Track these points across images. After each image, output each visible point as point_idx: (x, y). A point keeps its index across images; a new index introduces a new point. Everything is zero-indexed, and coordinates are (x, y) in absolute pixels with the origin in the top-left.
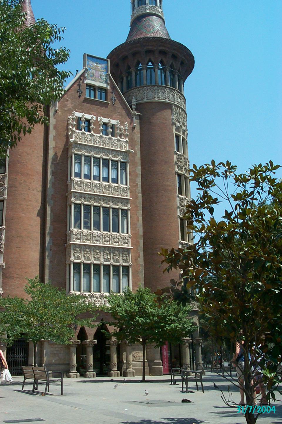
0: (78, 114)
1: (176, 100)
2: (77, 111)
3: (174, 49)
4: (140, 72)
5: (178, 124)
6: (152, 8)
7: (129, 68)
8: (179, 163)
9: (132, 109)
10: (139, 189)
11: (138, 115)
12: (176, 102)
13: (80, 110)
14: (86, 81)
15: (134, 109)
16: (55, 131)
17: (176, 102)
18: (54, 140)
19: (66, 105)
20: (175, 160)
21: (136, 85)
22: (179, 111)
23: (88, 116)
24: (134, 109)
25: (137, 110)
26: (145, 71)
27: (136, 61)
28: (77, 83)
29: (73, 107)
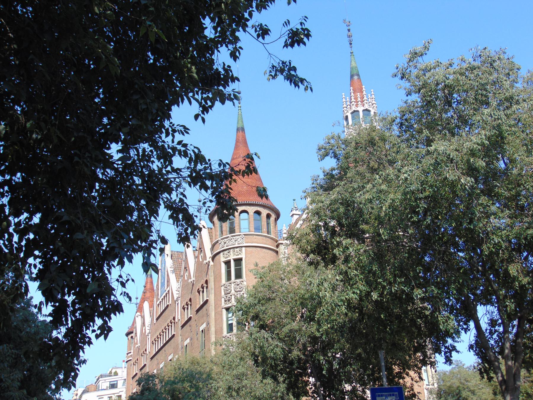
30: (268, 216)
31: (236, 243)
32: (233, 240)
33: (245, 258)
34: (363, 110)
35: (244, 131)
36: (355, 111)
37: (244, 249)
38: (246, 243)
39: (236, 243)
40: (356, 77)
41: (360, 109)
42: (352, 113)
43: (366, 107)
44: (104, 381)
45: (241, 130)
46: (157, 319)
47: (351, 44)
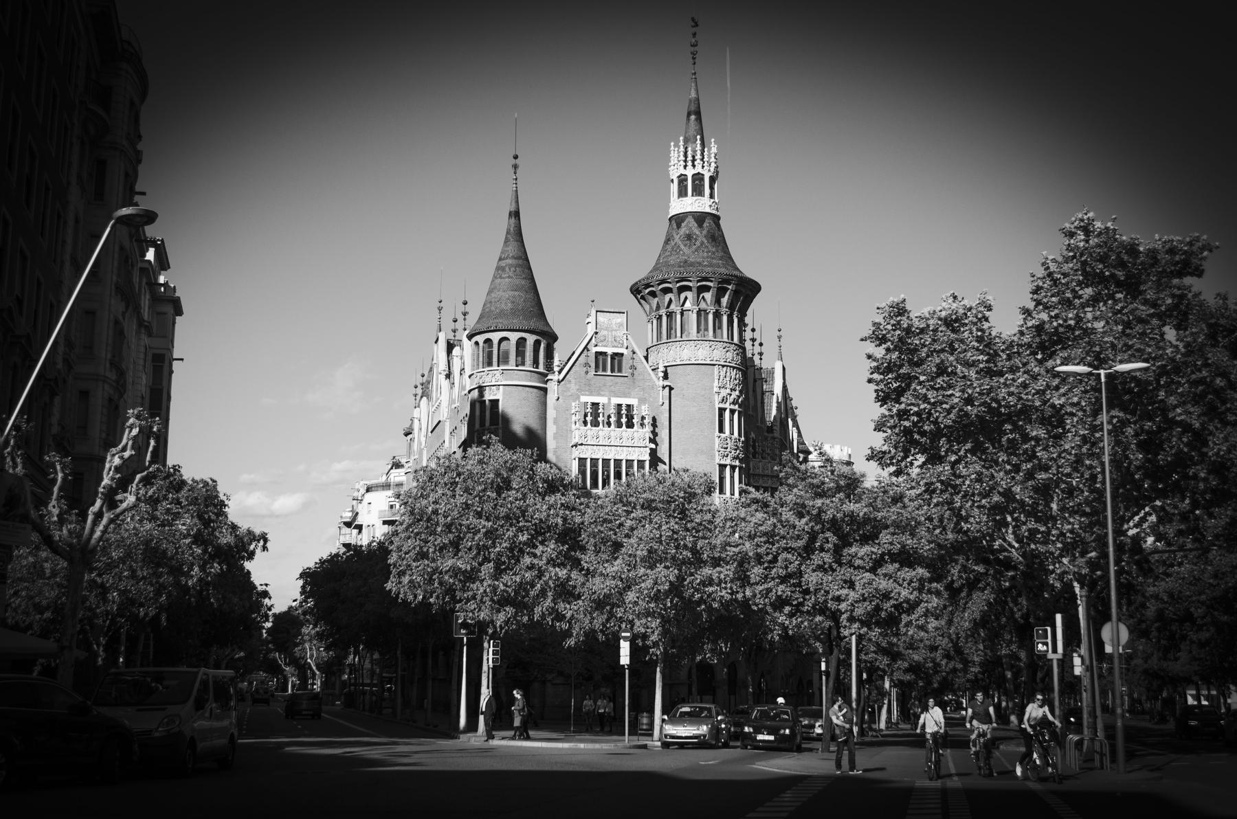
0: (584, 399)
2: (583, 395)
5: (724, 392)
7: (658, 308)
13: (587, 393)
16: (555, 427)
18: (555, 438)
19: (568, 390)
23: (596, 399)
24: (661, 378)
28: (583, 355)
30: (537, 343)
31: (493, 380)
32: (490, 376)
33: (504, 398)
34: (693, 175)
35: (519, 216)
36: (682, 175)
37: (501, 387)
38: (506, 380)
39: (493, 380)
40: (693, 117)
41: (690, 172)
42: (679, 177)
43: (699, 169)
44: (397, 474)
45: (516, 214)
46: (432, 432)
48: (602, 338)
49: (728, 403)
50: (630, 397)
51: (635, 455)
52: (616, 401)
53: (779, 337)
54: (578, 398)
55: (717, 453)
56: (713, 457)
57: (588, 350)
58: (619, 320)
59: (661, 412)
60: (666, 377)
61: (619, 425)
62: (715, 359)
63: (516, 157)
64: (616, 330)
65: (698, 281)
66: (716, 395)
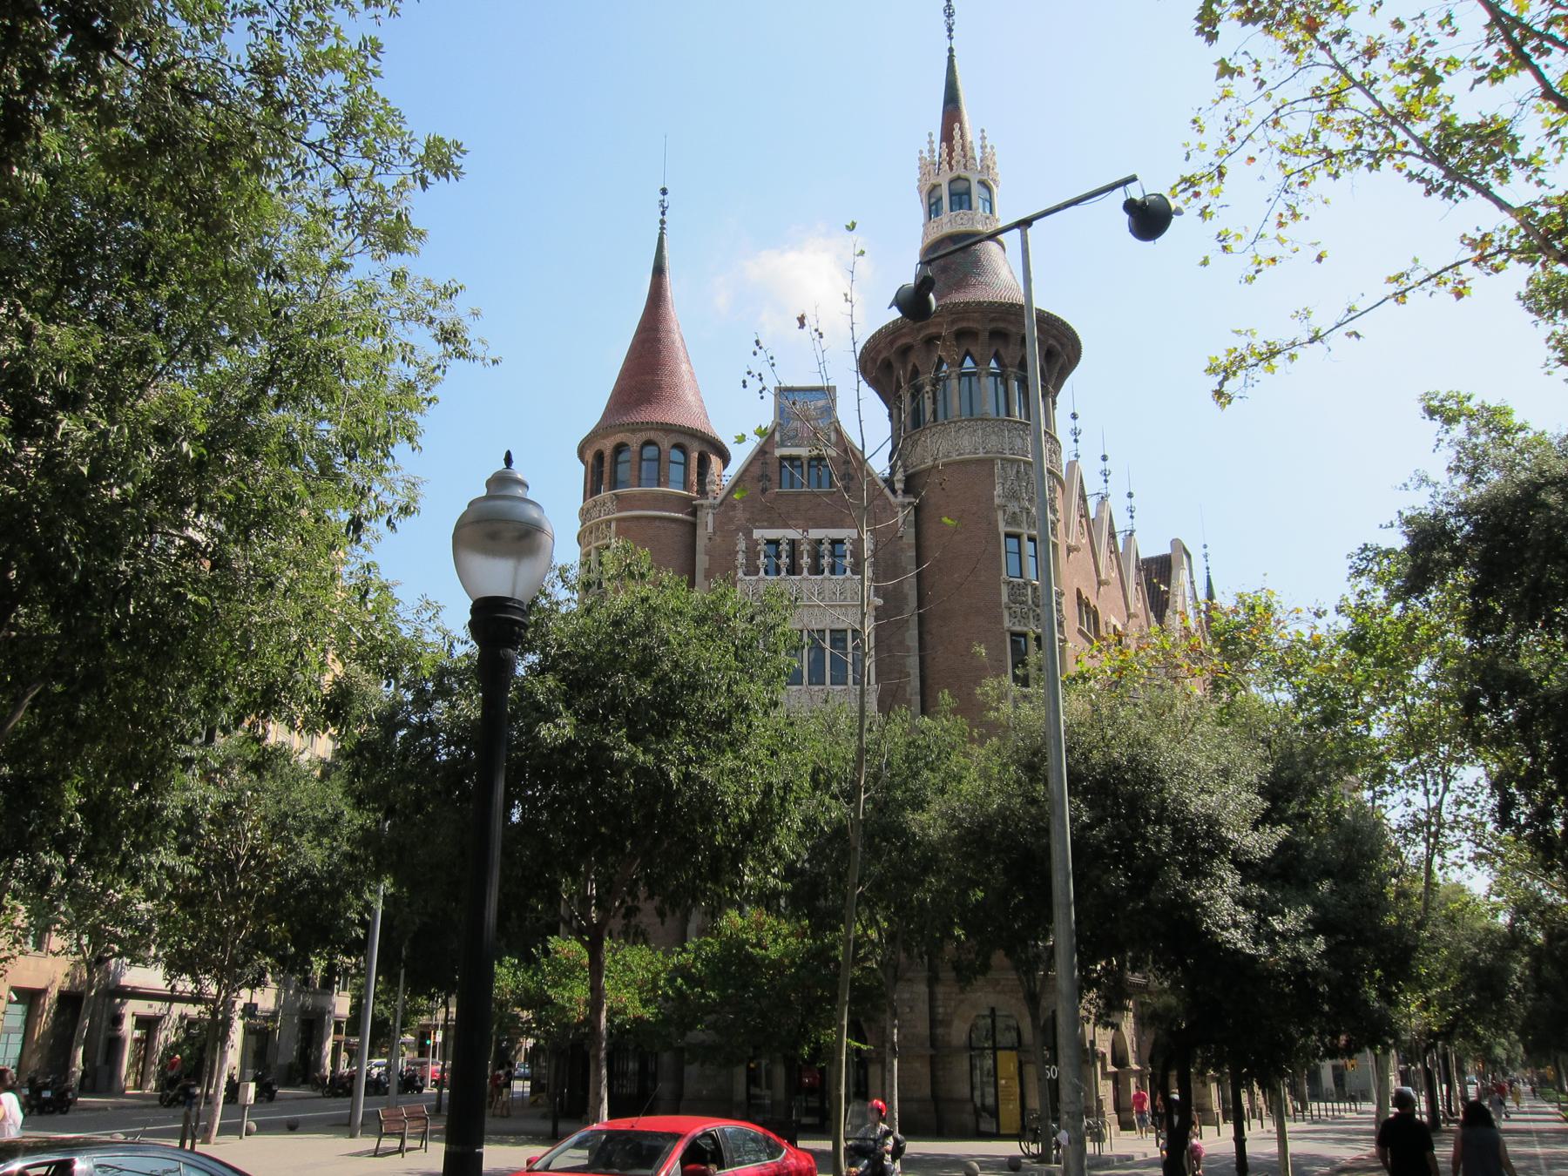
1: (1007, 447)
3: (993, 320)
4: (944, 385)
5: (1013, 507)
6: (958, 218)
8: (1016, 608)
9: (894, 492)
10: (912, 683)
11: (909, 504)
12: (1007, 451)
14: (778, 452)
15: (900, 492)
17: (1007, 451)
19: (731, 520)
20: (1005, 598)
21: (935, 420)
22: (1018, 472)
24: (900, 492)
25: (906, 492)
26: (954, 382)
27: (910, 367)
29: (748, 520)
34: (951, 182)
38: (619, 511)
43: (959, 171)
47: (950, 30)
48: (791, 434)
49: (1025, 525)
50: (843, 527)
51: (847, 621)
52: (815, 534)
53: (1206, 556)
54: (748, 534)
55: (1006, 614)
56: (999, 619)
57: (766, 453)
58: (821, 403)
59: (902, 550)
60: (906, 492)
61: (816, 569)
62: (995, 449)
63: (664, 192)
64: (817, 419)
65: (953, 322)
66: (1000, 514)
